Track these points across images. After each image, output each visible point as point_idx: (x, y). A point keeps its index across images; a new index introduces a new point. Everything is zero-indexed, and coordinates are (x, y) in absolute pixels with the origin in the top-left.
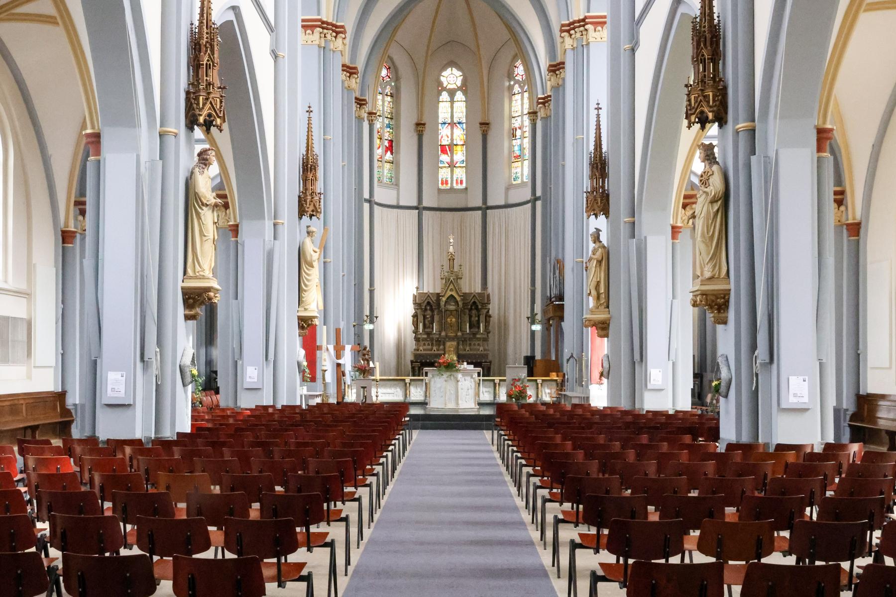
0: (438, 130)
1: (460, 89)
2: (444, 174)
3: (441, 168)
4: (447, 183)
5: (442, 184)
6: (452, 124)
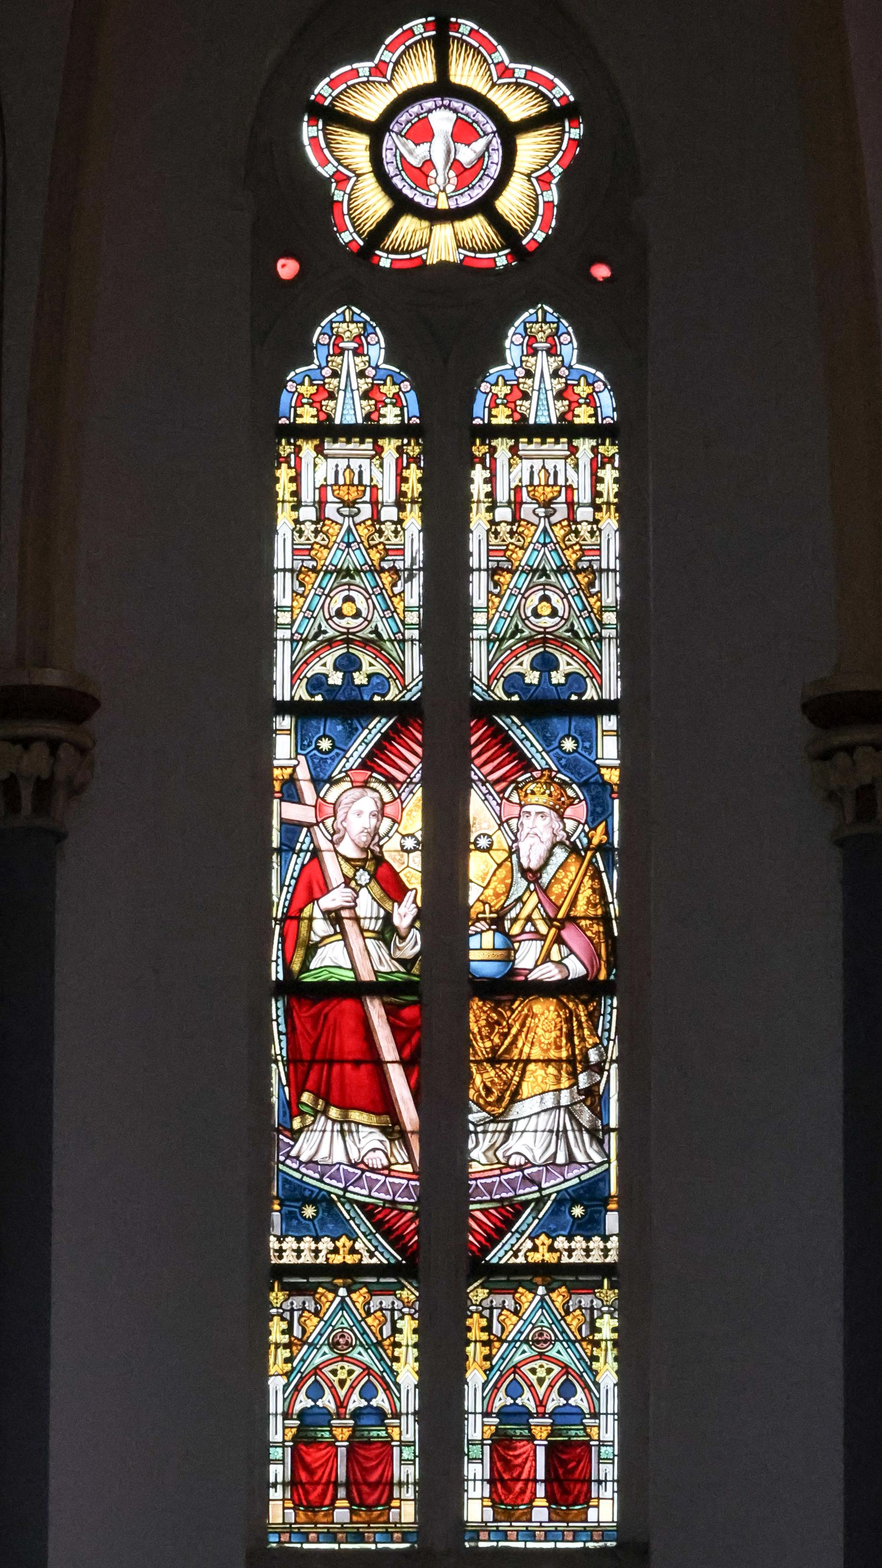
0: (259, 786)
1: (531, 274)
2: (332, 1358)
3: (303, 1279)
4: (369, 1484)
5: (307, 1490)
6: (449, 731)
